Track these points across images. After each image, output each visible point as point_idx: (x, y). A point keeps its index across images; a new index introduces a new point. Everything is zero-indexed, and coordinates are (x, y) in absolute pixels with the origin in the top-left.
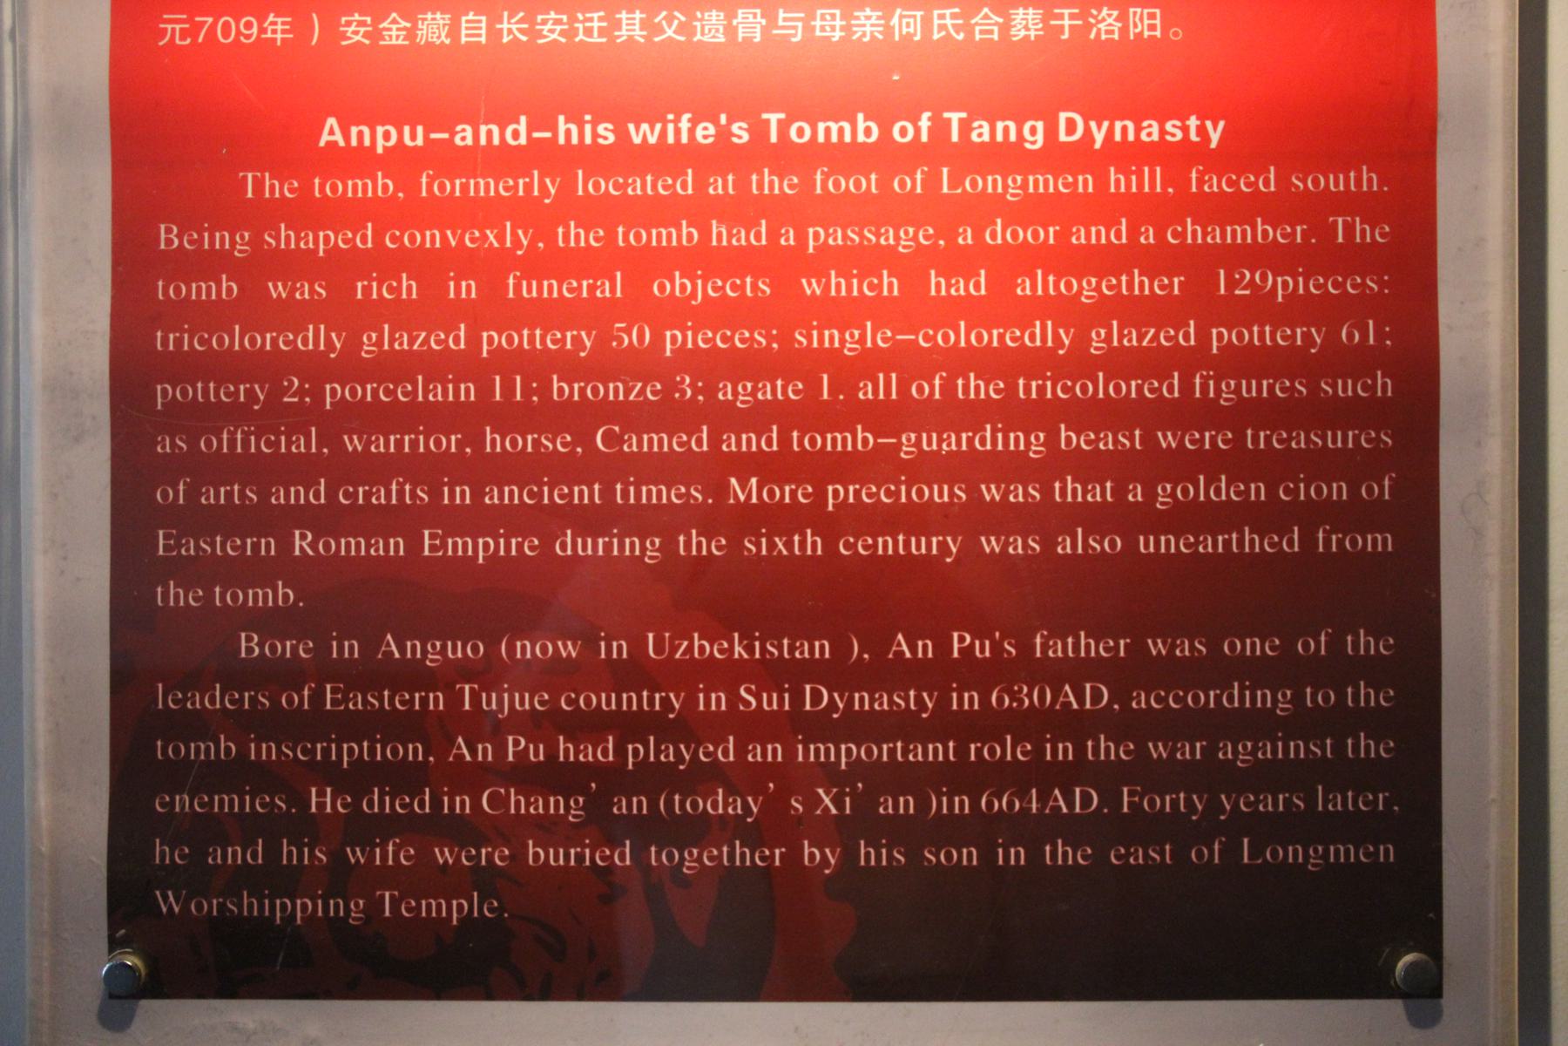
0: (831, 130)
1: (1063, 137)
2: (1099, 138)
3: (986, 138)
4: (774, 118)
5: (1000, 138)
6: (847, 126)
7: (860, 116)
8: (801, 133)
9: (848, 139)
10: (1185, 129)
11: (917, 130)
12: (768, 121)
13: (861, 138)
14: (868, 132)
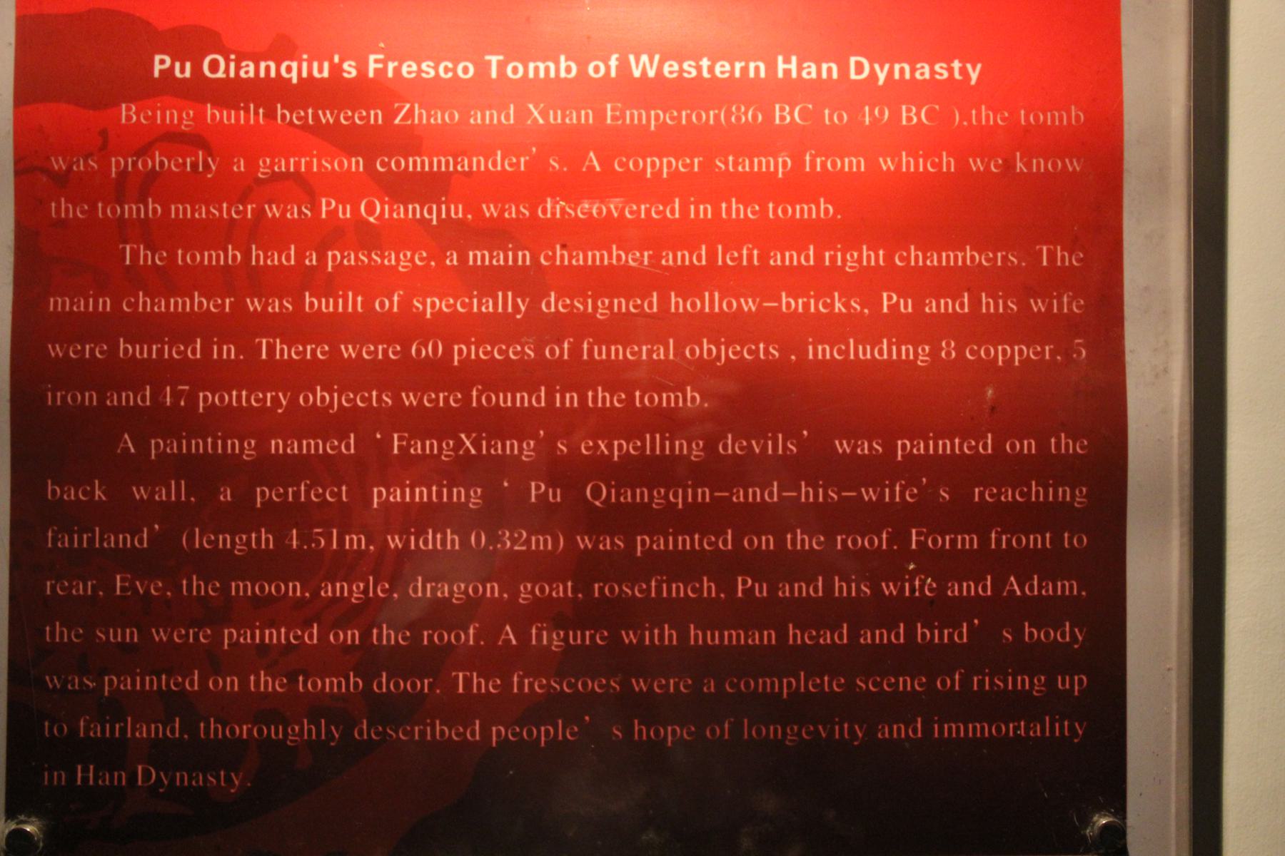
0: (539, 69)
1: (853, 76)
2: (882, 77)
3: (814, 75)
4: (494, 59)
5: (824, 75)
6: (552, 66)
7: (562, 58)
8: (515, 70)
9: (552, 75)
10: (950, 70)
11: (608, 68)
12: (489, 62)
13: (563, 74)
14: (568, 70)
